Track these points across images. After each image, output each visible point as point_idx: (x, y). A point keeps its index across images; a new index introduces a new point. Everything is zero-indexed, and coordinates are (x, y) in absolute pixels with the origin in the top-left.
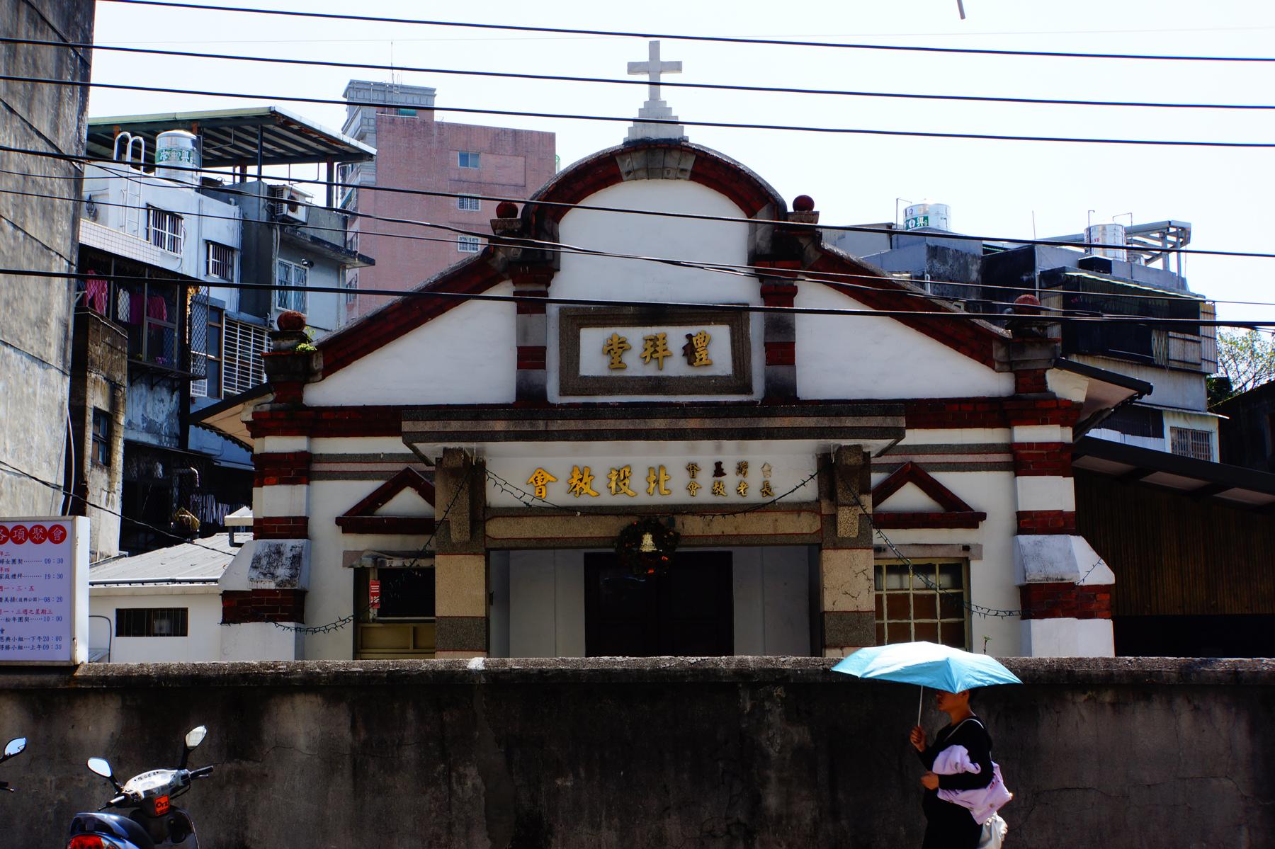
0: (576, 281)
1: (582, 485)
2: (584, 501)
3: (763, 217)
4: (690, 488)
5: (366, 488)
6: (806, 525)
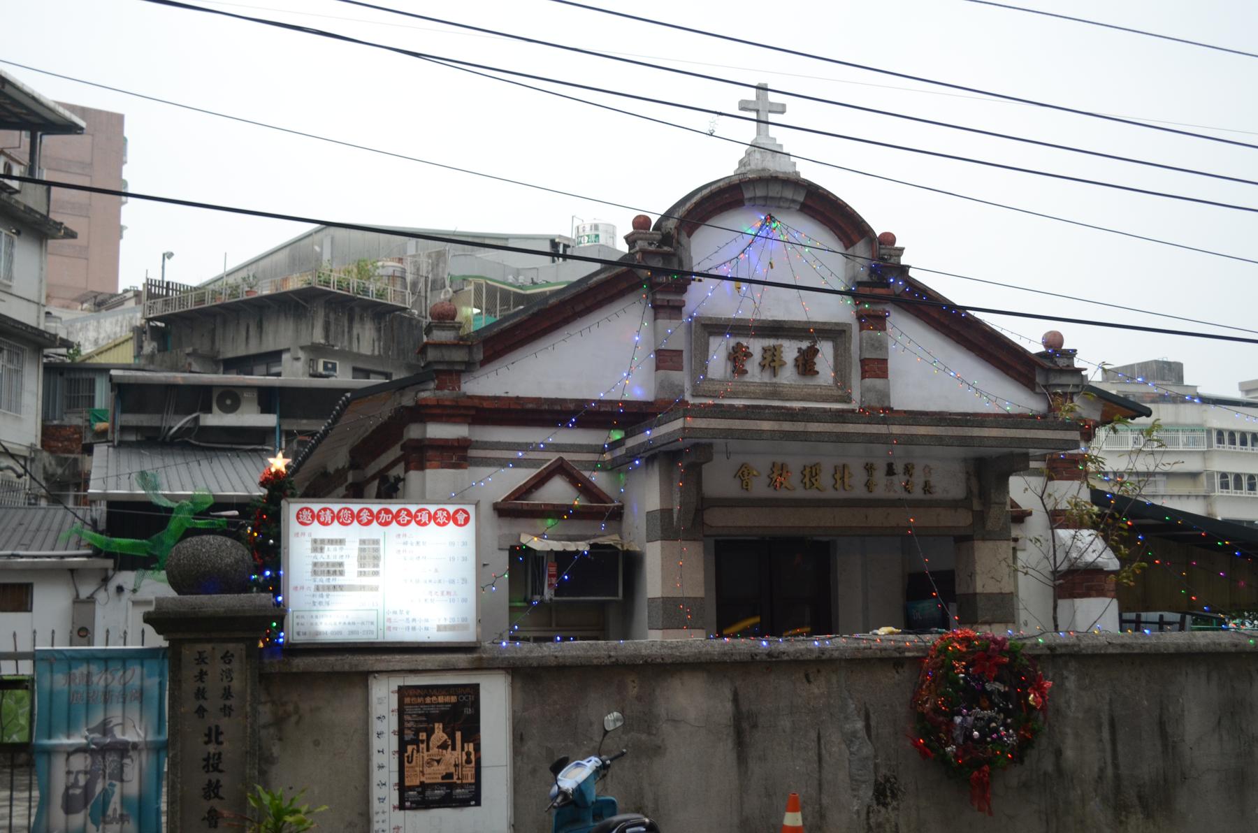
5: (522, 476)
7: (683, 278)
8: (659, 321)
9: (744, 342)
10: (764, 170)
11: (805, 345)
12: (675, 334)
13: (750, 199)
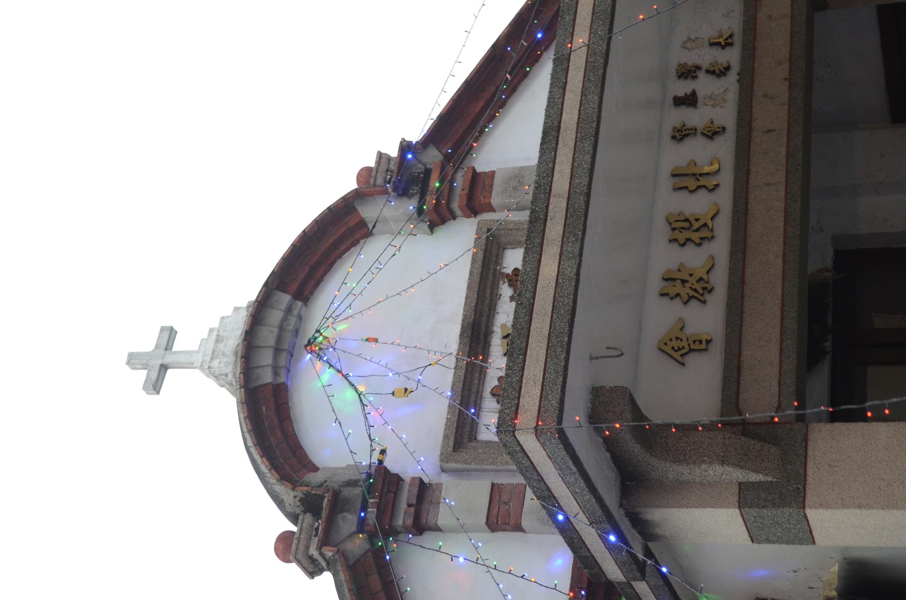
1: (692, 280)
2: (720, 279)
3: (368, 212)
4: (712, 133)
7: (382, 482)
8: (441, 522)
9: (491, 382)
10: (236, 353)
11: (506, 291)
12: (462, 498)
13: (276, 374)
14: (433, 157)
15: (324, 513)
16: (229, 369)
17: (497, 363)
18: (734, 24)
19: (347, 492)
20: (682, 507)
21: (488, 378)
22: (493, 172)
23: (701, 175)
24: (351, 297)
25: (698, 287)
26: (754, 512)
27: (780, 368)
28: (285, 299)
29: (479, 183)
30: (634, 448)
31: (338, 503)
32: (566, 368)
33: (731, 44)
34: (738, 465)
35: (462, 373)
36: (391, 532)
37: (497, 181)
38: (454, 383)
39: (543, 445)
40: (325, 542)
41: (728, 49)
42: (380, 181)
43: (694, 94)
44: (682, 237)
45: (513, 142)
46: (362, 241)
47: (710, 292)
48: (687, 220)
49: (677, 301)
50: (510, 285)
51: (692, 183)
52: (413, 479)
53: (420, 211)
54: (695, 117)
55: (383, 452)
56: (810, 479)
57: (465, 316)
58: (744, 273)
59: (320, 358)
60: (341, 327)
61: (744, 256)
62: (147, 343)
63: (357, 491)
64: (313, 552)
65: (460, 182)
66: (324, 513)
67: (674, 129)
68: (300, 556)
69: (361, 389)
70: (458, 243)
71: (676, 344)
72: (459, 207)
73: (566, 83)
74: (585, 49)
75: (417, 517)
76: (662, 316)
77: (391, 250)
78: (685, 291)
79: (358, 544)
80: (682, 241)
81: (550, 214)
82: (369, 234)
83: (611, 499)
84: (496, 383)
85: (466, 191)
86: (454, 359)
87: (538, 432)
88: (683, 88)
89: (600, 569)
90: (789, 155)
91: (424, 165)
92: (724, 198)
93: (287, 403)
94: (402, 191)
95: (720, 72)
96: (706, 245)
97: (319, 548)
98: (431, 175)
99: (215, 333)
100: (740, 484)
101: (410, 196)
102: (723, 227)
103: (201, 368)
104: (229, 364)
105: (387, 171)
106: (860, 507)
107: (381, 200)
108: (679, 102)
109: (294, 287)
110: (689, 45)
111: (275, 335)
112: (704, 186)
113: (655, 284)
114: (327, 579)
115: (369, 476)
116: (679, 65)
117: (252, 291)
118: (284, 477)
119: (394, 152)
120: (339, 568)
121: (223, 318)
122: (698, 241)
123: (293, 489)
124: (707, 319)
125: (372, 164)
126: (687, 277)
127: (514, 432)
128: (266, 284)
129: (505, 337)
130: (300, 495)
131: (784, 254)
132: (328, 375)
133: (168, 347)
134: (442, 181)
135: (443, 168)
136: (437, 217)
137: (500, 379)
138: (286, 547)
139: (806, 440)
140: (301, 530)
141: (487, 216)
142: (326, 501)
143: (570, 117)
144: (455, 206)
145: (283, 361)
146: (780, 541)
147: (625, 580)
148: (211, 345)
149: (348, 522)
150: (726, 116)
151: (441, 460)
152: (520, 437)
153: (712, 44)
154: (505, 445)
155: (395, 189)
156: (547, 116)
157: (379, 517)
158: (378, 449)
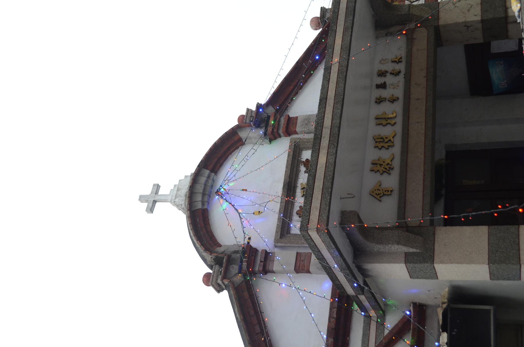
0: (262, 233)
1: (384, 164)
2: (396, 163)
3: (243, 134)
4: (393, 100)
6: (422, 37)
7: (249, 251)
8: (275, 269)
9: (296, 208)
10: (186, 196)
11: (303, 169)
12: (284, 258)
13: (203, 205)
14: (271, 110)
15: (224, 265)
16: (183, 203)
17: (299, 201)
18: (402, 53)
19: (234, 256)
20: (380, 263)
21: (295, 207)
22: (297, 118)
23: (388, 118)
24: (235, 171)
25: (387, 167)
26: (411, 265)
27: (423, 202)
28: (207, 172)
29: (291, 122)
30: (360, 238)
31: (230, 261)
32: (330, 203)
33: (401, 62)
34: (405, 245)
35: (284, 204)
36: (253, 274)
37: (299, 121)
38: (280, 209)
39: (320, 236)
40: (224, 278)
41: (399, 63)
42: (248, 121)
43: (385, 83)
44: (380, 146)
45: (307, 103)
46: (240, 147)
47: (392, 169)
48: (382, 138)
49: (378, 174)
50: (304, 166)
51: (384, 122)
52: (263, 250)
53: (265, 134)
54: (385, 93)
55: (249, 239)
56: (436, 251)
57: (285, 179)
58: (407, 161)
59: (222, 197)
60: (231, 184)
61: (407, 154)
62: (148, 191)
63: (238, 255)
64: (219, 281)
65: (283, 121)
66: (224, 265)
67: (376, 98)
68: (213, 283)
69: (240, 211)
70: (281, 148)
71: (378, 192)
72: (283, 132)
73: (329, 79)
74: (338, 64)
75: (264, 266)
76: (371, 180)
77: (253, 151)
78: (381, 169)
79: (239, 278)
80: (380, 147)
81: (323, 136)
82: (243, 144)
83: (350, 260)
84: (298, 209)
85: (286, 125)
86: (280, 199)
87: (318, 230)
88: (380, 80)
89: (344, 290)
90: (426, 110)
91: (267, 114)
92: (398, 128)
93: (208, 217)
94: (258, 125)
95: (396, 74)
96: (390, 149)
97: (222, 280)
98: (270, 119)
99: (177, 187)
100: (406, 253)
101: (261, 128)
102: (398, 141)
103: (171, 202)
104: (183, 200)
105: (251, 116)
106: (458, 263)
107: (248, 130)
108: (378, 86)
109: (211, 167)
110: (382, 62)
111: (202, 188)
112: (390, 123)
113: (368, 166)
114: (225, 294)
115: (243, 248)
116: (379, 71)
117: (192, 169)
118: (207, 249)
119: (254, 109)
120: (231, 289)
121: (180, 180)
122: (387, 147)
123: (211, 254)
124: (391, 181)
125: (245, 114)
126: (382, 163)
127: (307, 230)
128: (199, 166)
129: (302, 189)
130: (214, 257)
131: (425, 153)
132: (225, 205)
133: (157, 193)
134: (275, 121)
135: (275, 115)
136: (272, 136)
137: (300, 207)
138: (207, 279)
139: (434, 234)
140: (214, 272)
141: (294, 136)
142: (225, 259)
143: (331, 94)
144: (281, 132)
145: (206, 199)
146: (423, 278)
147: (355, 294)
148: (175, 192)
149: (234, 269)
150: (399, 93)
151: (275, 242)
152: (310, 232)
153: (393, 62)
154: (303, 236)
155: (254, 125)
156: (321, 93)
157: (248, 267)
158: (247, 237)
